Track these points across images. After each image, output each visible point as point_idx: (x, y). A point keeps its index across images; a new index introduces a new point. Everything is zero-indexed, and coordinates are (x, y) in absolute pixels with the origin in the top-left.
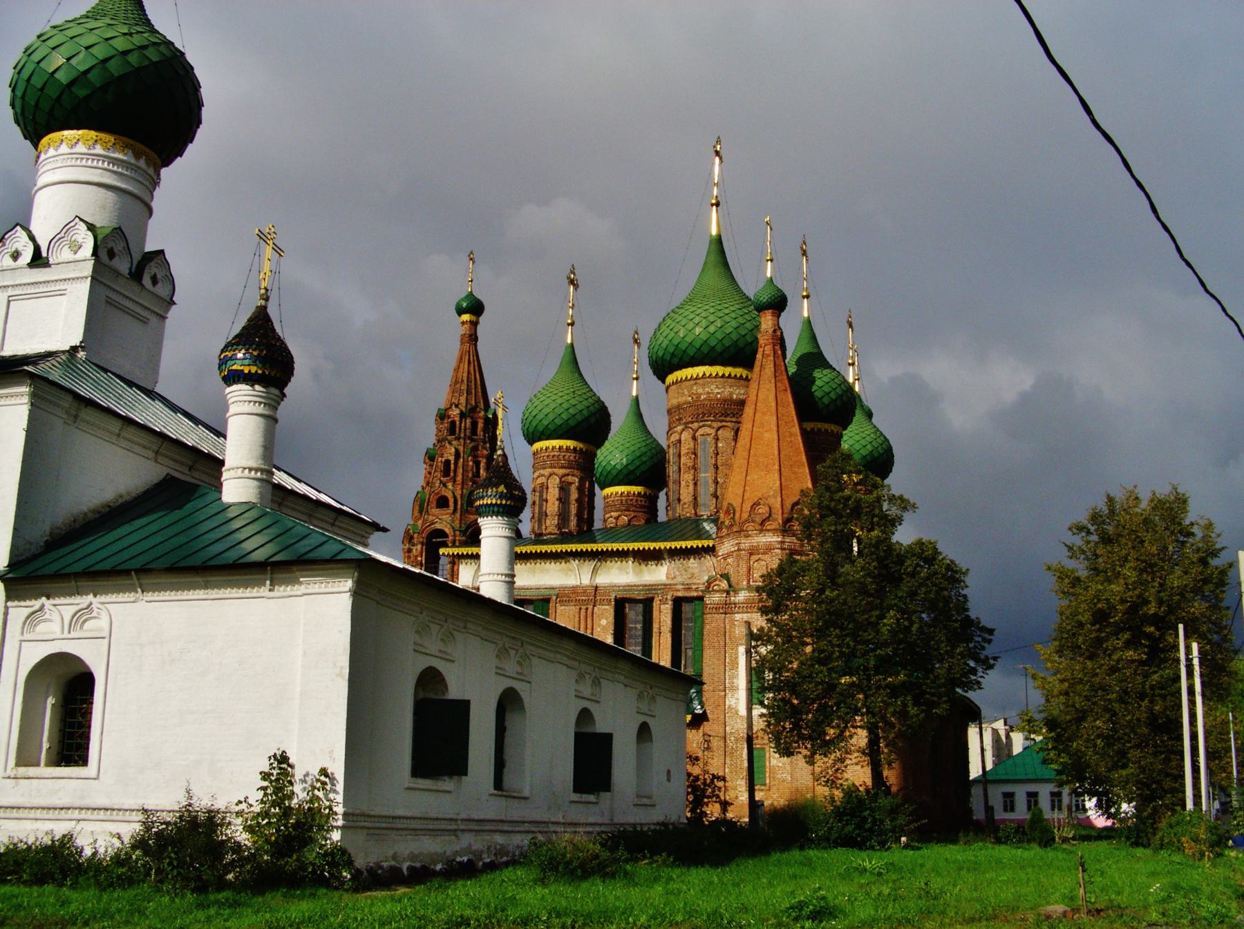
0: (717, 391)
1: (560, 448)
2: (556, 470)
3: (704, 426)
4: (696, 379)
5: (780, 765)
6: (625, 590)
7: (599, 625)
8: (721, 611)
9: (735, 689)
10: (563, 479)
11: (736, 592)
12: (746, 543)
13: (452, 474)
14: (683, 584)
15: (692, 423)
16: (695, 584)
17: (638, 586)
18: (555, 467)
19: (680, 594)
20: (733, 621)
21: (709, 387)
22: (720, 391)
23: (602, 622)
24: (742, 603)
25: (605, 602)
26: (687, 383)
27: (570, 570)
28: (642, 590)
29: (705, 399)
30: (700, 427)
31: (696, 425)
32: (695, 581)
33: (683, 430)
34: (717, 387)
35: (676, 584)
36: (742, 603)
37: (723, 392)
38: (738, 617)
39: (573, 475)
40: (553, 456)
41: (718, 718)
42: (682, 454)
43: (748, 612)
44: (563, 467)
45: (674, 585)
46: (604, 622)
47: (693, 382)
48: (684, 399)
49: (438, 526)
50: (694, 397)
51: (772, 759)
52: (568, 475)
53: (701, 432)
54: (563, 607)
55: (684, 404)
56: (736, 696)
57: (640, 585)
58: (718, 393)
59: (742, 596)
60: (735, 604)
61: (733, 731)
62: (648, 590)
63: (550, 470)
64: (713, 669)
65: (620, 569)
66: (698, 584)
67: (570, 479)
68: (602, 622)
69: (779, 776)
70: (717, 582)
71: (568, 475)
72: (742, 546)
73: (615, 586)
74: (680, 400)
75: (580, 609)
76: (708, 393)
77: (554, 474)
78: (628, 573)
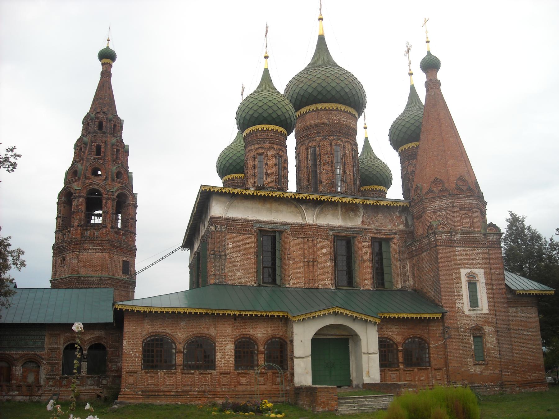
0: (343, 119)
2: (273, 146)
3: (337, 139)
4: (331, 110)
5: (493, 347)
6: (338, 230)
7: (322, 253)
8: (447, 245)
9: (460, 296)
11: (456, 233)
12: (458, 203)
13: (102, 154)
14: (377, 230)
15: (330, 136)
16: (384, 230)
17: (347, 228)
19: (374, 236)
20: (455, 251)
21: (339, 116)
22: (345, 120)
23: (323, 251)
24: (459, 241)
25: (325, 237)
26: (325, 112)
27: (298, 213)
28: (350, 231)
29: (337, 123)
30: (335, 139)
31: (331, 138)
32: (383, 228)
33: (323, 139)
34: (344, 118)
35: (373, 229)
36: (459, 241)
37: (347, 121)
38: (457, 249)
39: (283, 151)
41: (453, 316)
42: (322, 153)
43: (464, 247)
45: (371, 229)
46: (324, 251)
47: (329, 112)
48: (323, 121)
49: (95, 187)
50: (331, 121)
51: (487, 344)
52: (279, 150)
53: (335, 142)
54: (294, 238)
55: (322, 124)
56: (461, 301)
57: (349, 228)
58: (344, 121)
59: (459, 236)
60: (455, 241)
61: (462, 325)
62: (353, 231)
63: (268, 145)
64: (447, 283)
65: (333, 215)
66: (386, 230)
68: (323, 251)
69: (493, 354)
70: (442, 226)
71: (279, 150)
72: (455, 204)
73: (332, 227)
74: (319, 121)
76: (339, 120)
77: (272, 148)
78: (338, 219)
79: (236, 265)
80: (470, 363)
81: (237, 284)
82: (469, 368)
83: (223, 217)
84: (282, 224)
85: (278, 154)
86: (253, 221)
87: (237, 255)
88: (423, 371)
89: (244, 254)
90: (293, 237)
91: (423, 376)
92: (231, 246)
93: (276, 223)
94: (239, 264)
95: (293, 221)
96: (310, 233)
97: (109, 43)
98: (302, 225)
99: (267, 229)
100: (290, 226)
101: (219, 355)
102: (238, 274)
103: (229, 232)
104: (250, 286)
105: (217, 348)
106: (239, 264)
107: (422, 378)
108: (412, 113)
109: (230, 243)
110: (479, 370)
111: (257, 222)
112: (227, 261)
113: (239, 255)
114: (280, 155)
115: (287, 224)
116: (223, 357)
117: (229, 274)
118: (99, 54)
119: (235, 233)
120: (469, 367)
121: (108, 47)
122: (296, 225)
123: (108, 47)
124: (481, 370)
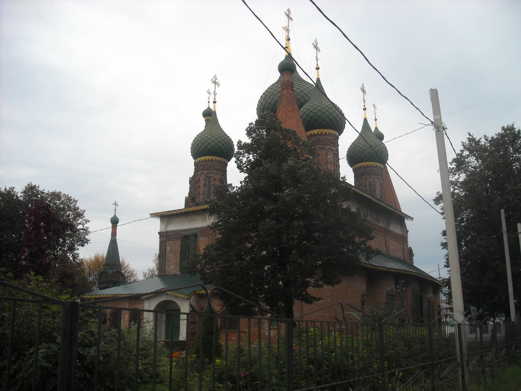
1: (212, 160)
10: (207, 175)
18: (203, 170)
39: (211, 173)
40: (203, 165)
44: (206, 170)
52: (209, 173)
54: (202, 238)
63: (201, 172)
67: (210, 175)
71: (209, 173)
75: (209, 238)
79: (170, 262)
80: (266, 328)
81: (170, 274)
82: (265, 332)
83: (164, 231)
84: (195, 229)
85: (207, 177)
86: (179, 230)
87: (171, 255)
88: (234, 333)
89: (175, 254)
90: (201, 237)
91: (234, 337)
92: (168, 250)
93: (191, 229)
94: (172, 261)
95: (202, 226)
96: (211, 232)
97: (209, 104)
98: (205, 228)
99: (187, 234)
100: (201, 230)
101: (122, 321)
102: (172, 267)
103: (167, 241)
104: (177, 275)
105: (122, 317)
106: (172, 261)
107: (233, 339)
108: (315, 103)
109: (168, 248)
110: (273, 334)
111: (181, 231)
112: (166, 259)
113: (172, 255)
114: (209, 177)
115: (197, 229)
116: (124, 322)
117: (167, 268)
118: (203, 114)
119: (171, 241)
120: (265, 331)
121: (209, 108)
122: (203, 228)
123: (209, 108)
124: (274, 334)
